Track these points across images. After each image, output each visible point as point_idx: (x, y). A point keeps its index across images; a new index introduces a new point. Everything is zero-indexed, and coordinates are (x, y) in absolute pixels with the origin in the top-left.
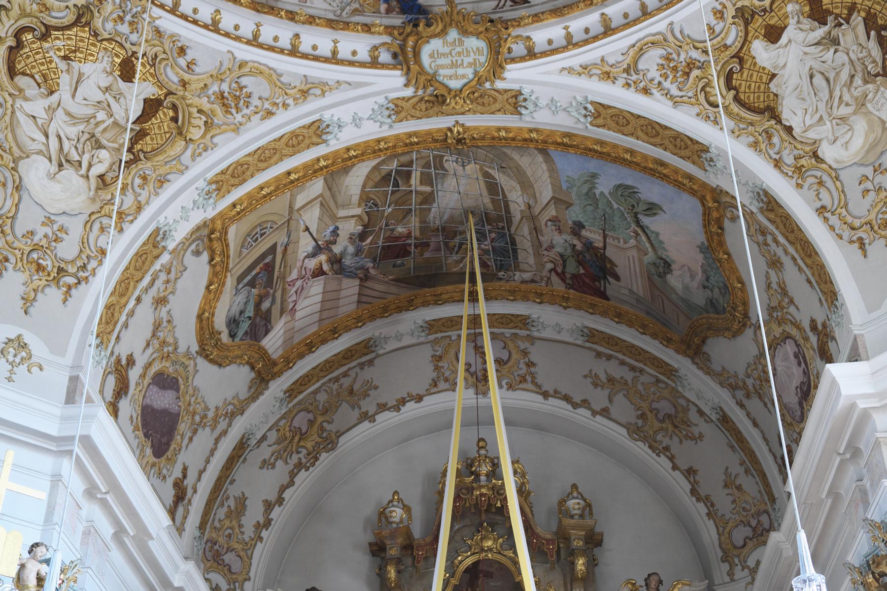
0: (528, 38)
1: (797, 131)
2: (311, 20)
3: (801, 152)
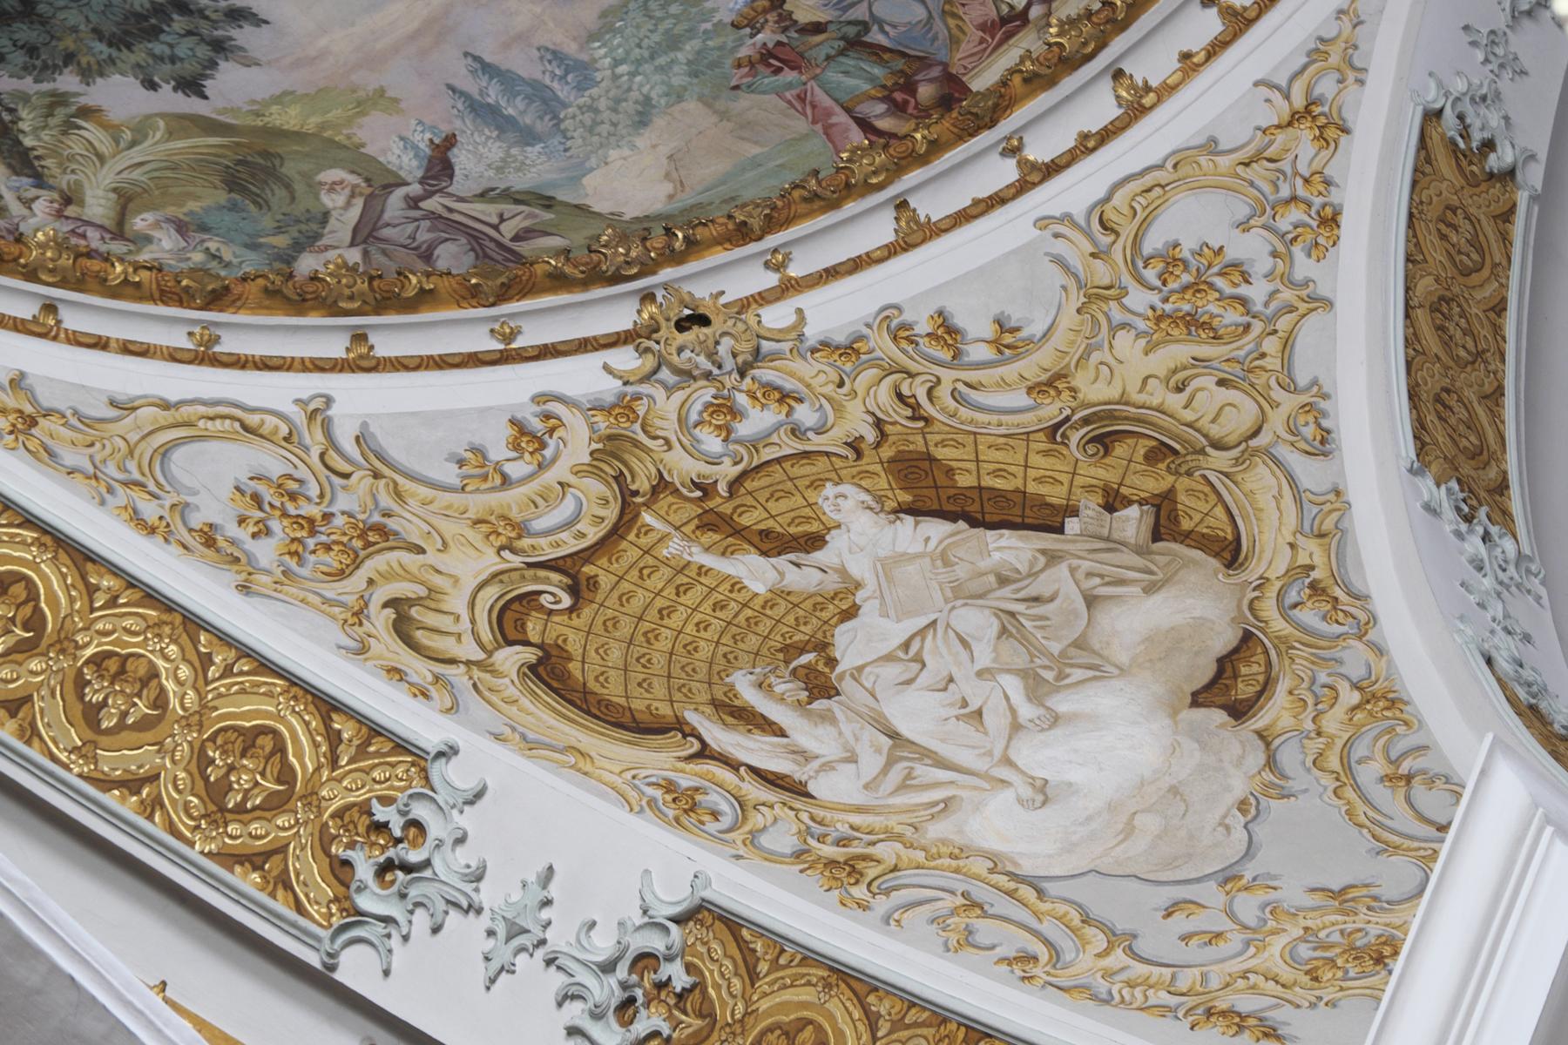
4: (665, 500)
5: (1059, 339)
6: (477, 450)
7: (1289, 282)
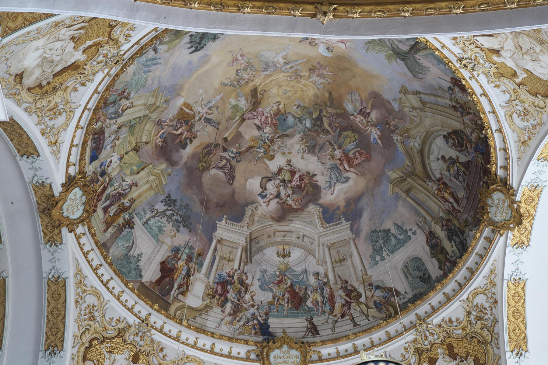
0: (319, 352)
2: (221, 337)
4: (106, 42)
5: (69, 94)
6: (133, 31)
7: (44, 123)
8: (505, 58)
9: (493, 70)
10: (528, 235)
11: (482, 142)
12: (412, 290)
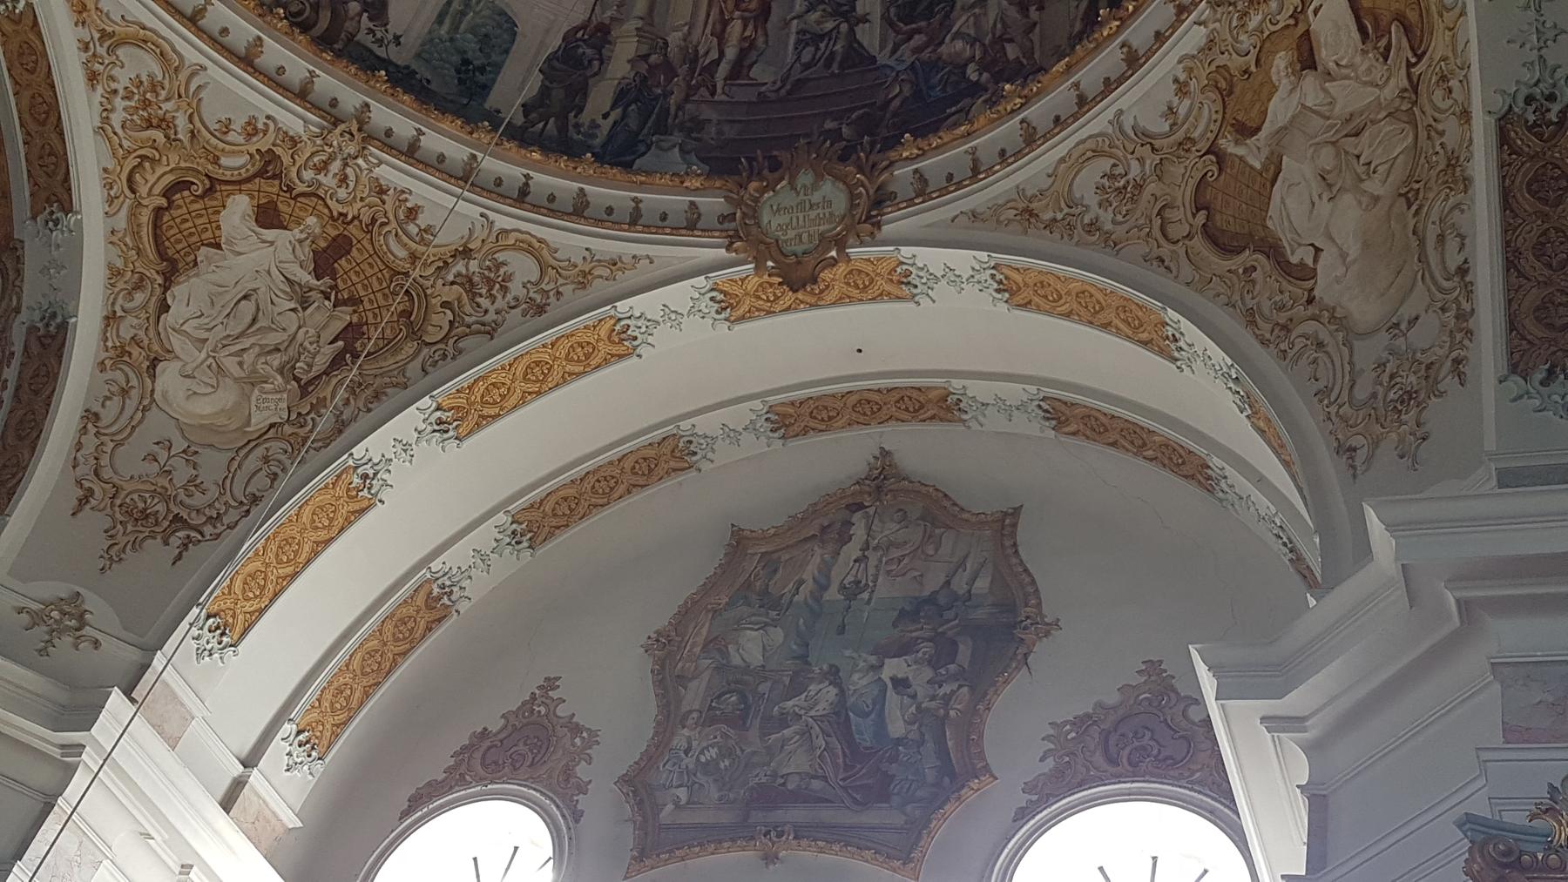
1: (169, 318)
3: (146, 342)
8: (1291, 91)
9: (1235, 63)
10: (758, 310)
11: (953, 78)
12: (418, 56)
